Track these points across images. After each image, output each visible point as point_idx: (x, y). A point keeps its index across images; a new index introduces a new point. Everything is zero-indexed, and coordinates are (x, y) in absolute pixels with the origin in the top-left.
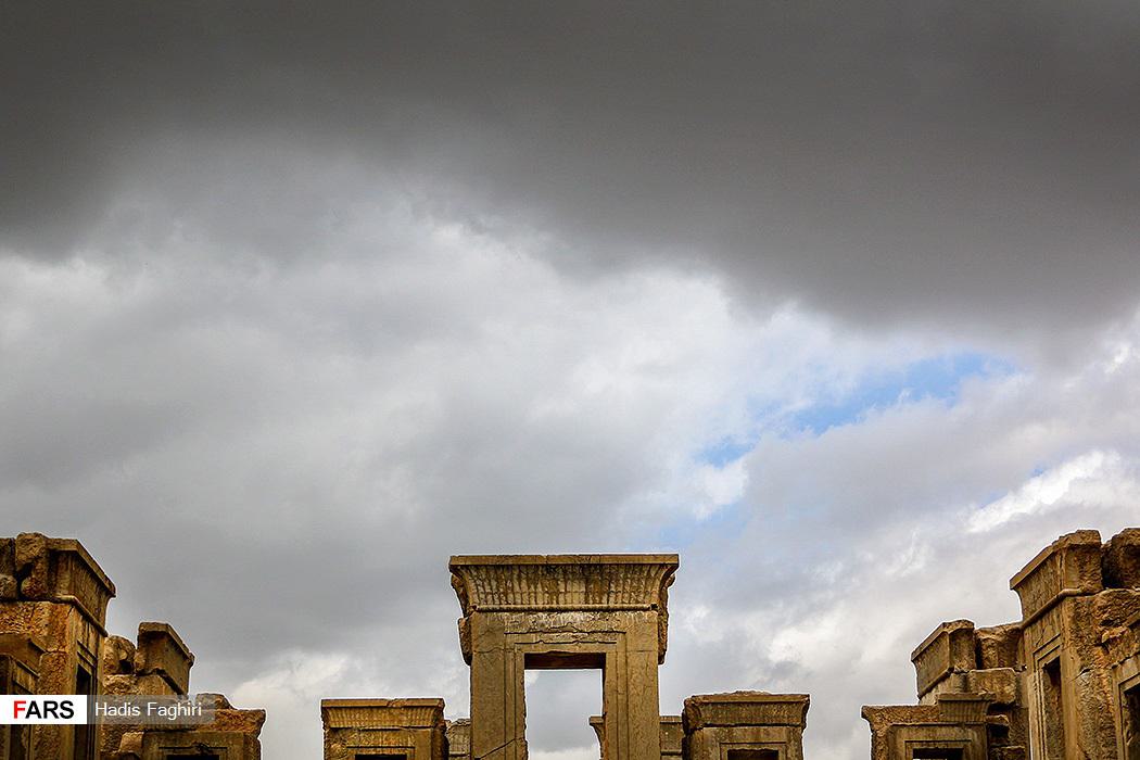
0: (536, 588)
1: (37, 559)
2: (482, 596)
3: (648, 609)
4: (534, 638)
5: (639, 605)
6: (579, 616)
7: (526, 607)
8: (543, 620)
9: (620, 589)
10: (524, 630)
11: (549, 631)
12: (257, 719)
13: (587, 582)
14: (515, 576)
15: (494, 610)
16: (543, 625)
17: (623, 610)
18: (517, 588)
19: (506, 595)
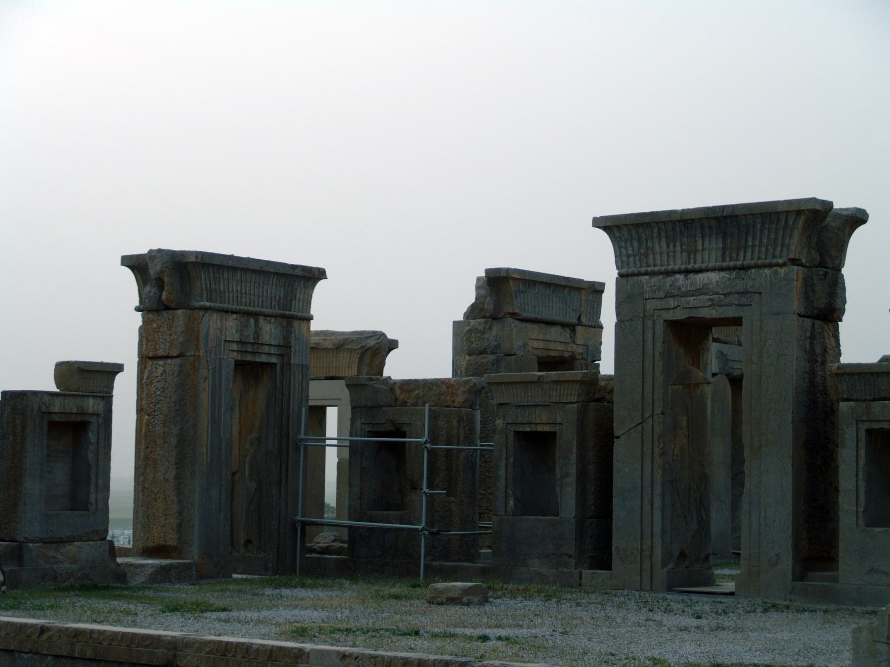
0: (675, 246)
1: (161, 272)
2: (625, 259)
3: (783, 265)
4: (672, 303)
5: (774, 261)
6: (714, 276)
7: (663, 269)
8: (680, 283)
9: (757, 243)
10: (662, 294)
11: (686, 294)
12: (468, 387)
13: (724, 236)
14: (655, 235)
15: (633, 275)
16: (679, 288)
17: (757, 266)
18: (657, 249)
19: (646, 255)
